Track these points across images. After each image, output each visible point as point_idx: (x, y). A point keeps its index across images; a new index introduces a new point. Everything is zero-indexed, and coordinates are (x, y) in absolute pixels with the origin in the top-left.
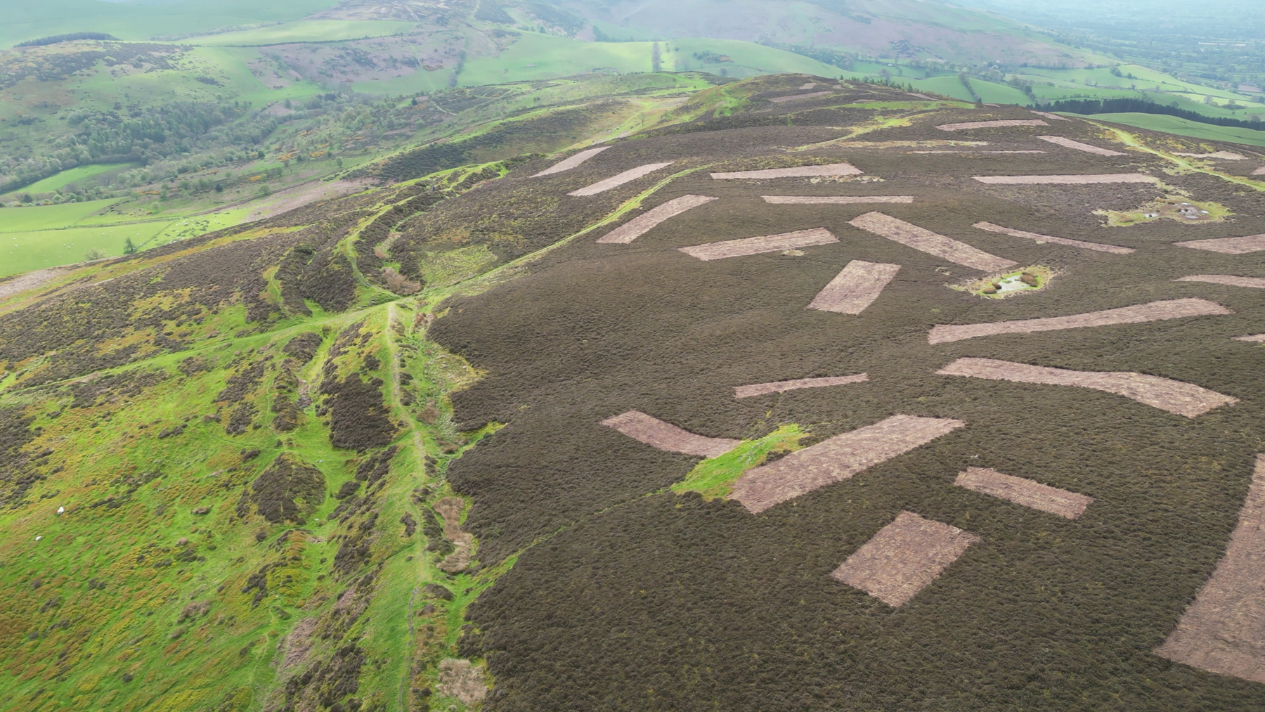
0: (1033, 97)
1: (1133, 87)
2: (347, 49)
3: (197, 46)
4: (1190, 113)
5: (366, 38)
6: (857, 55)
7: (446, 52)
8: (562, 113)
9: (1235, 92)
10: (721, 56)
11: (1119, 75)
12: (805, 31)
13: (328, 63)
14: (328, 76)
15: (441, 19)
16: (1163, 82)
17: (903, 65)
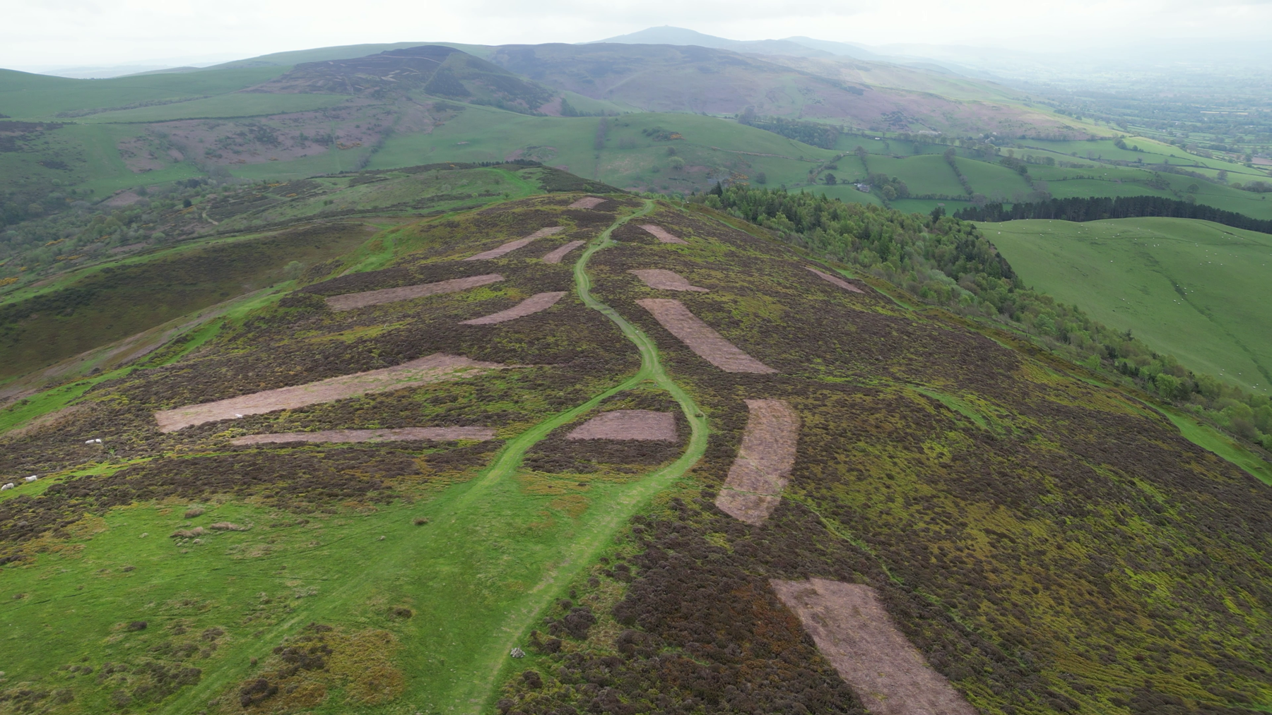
0: (1028, 180)
1: (1140, 161)
2: (254, 125)
3: (72, 123)
4: (1231, 214)
5: (283, 113)
6: (842, 128)
7: (369, 129)
8: (222, 250)
9: (1249, 166)
10: (672, 133)
11: (1123, 147)
12: (793, 102)
13: (220, 141)
14: (215, 156)
15: (376, 91)
16: (1172, 156)
17: (891, 139)
